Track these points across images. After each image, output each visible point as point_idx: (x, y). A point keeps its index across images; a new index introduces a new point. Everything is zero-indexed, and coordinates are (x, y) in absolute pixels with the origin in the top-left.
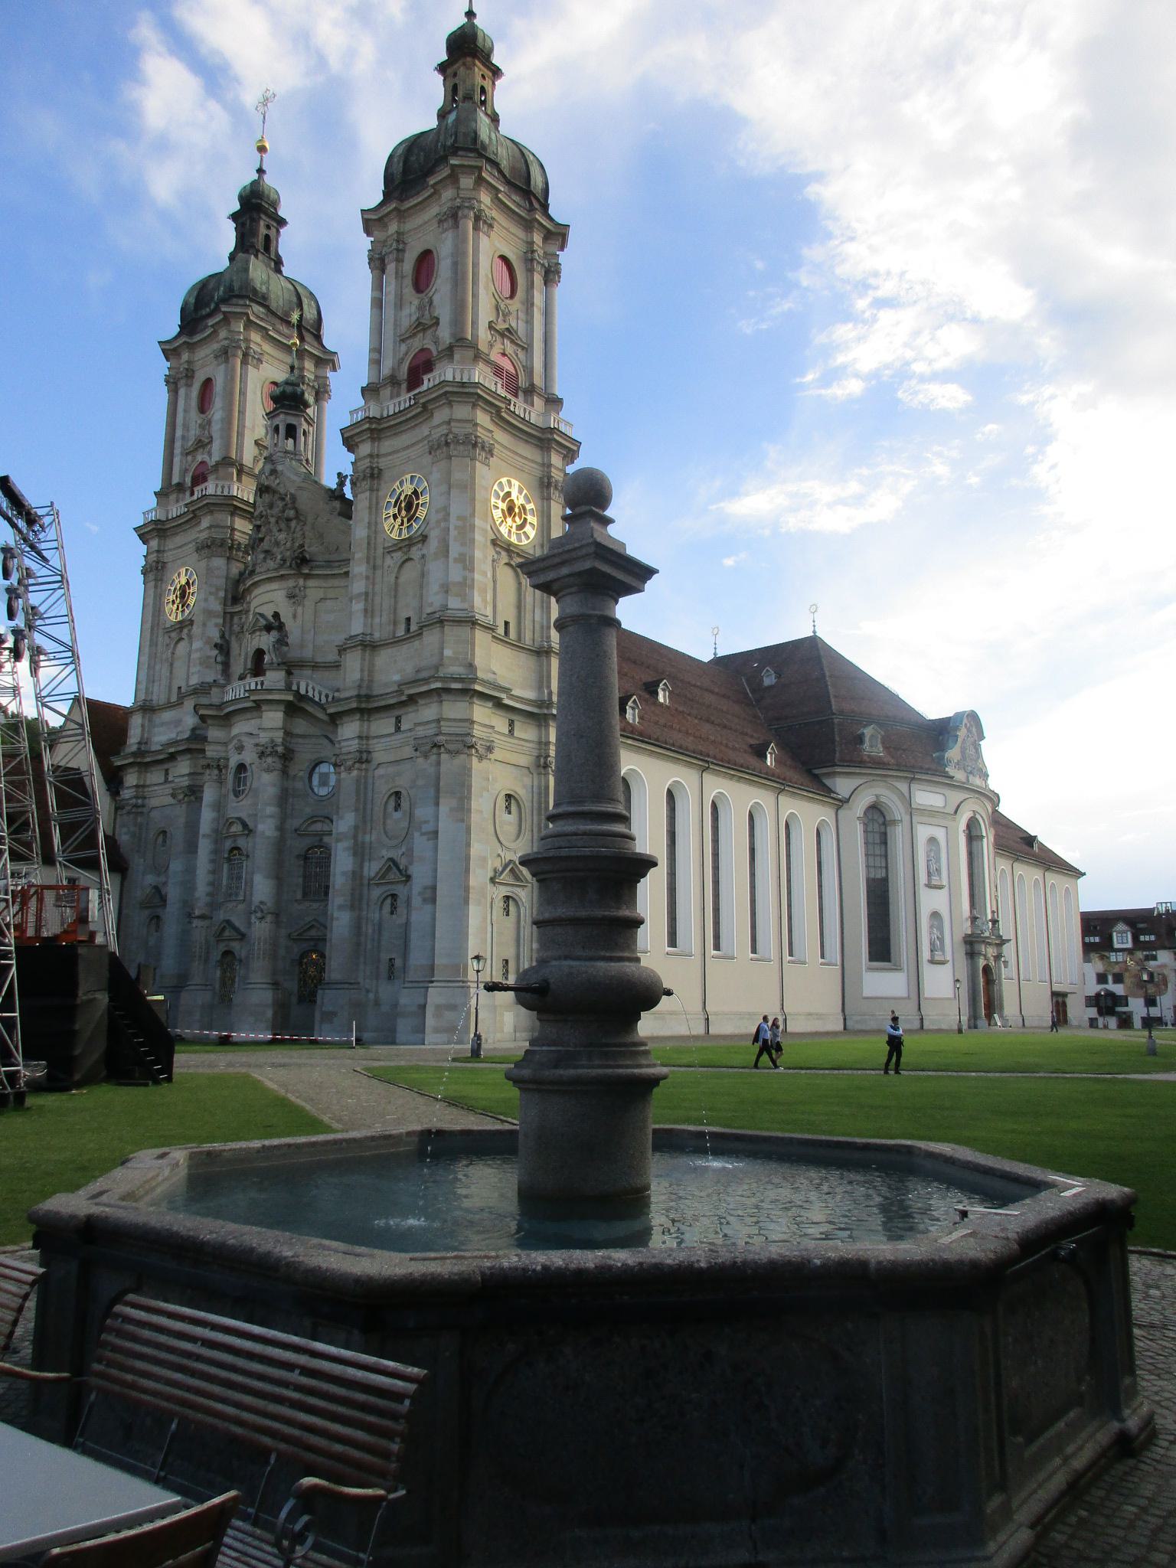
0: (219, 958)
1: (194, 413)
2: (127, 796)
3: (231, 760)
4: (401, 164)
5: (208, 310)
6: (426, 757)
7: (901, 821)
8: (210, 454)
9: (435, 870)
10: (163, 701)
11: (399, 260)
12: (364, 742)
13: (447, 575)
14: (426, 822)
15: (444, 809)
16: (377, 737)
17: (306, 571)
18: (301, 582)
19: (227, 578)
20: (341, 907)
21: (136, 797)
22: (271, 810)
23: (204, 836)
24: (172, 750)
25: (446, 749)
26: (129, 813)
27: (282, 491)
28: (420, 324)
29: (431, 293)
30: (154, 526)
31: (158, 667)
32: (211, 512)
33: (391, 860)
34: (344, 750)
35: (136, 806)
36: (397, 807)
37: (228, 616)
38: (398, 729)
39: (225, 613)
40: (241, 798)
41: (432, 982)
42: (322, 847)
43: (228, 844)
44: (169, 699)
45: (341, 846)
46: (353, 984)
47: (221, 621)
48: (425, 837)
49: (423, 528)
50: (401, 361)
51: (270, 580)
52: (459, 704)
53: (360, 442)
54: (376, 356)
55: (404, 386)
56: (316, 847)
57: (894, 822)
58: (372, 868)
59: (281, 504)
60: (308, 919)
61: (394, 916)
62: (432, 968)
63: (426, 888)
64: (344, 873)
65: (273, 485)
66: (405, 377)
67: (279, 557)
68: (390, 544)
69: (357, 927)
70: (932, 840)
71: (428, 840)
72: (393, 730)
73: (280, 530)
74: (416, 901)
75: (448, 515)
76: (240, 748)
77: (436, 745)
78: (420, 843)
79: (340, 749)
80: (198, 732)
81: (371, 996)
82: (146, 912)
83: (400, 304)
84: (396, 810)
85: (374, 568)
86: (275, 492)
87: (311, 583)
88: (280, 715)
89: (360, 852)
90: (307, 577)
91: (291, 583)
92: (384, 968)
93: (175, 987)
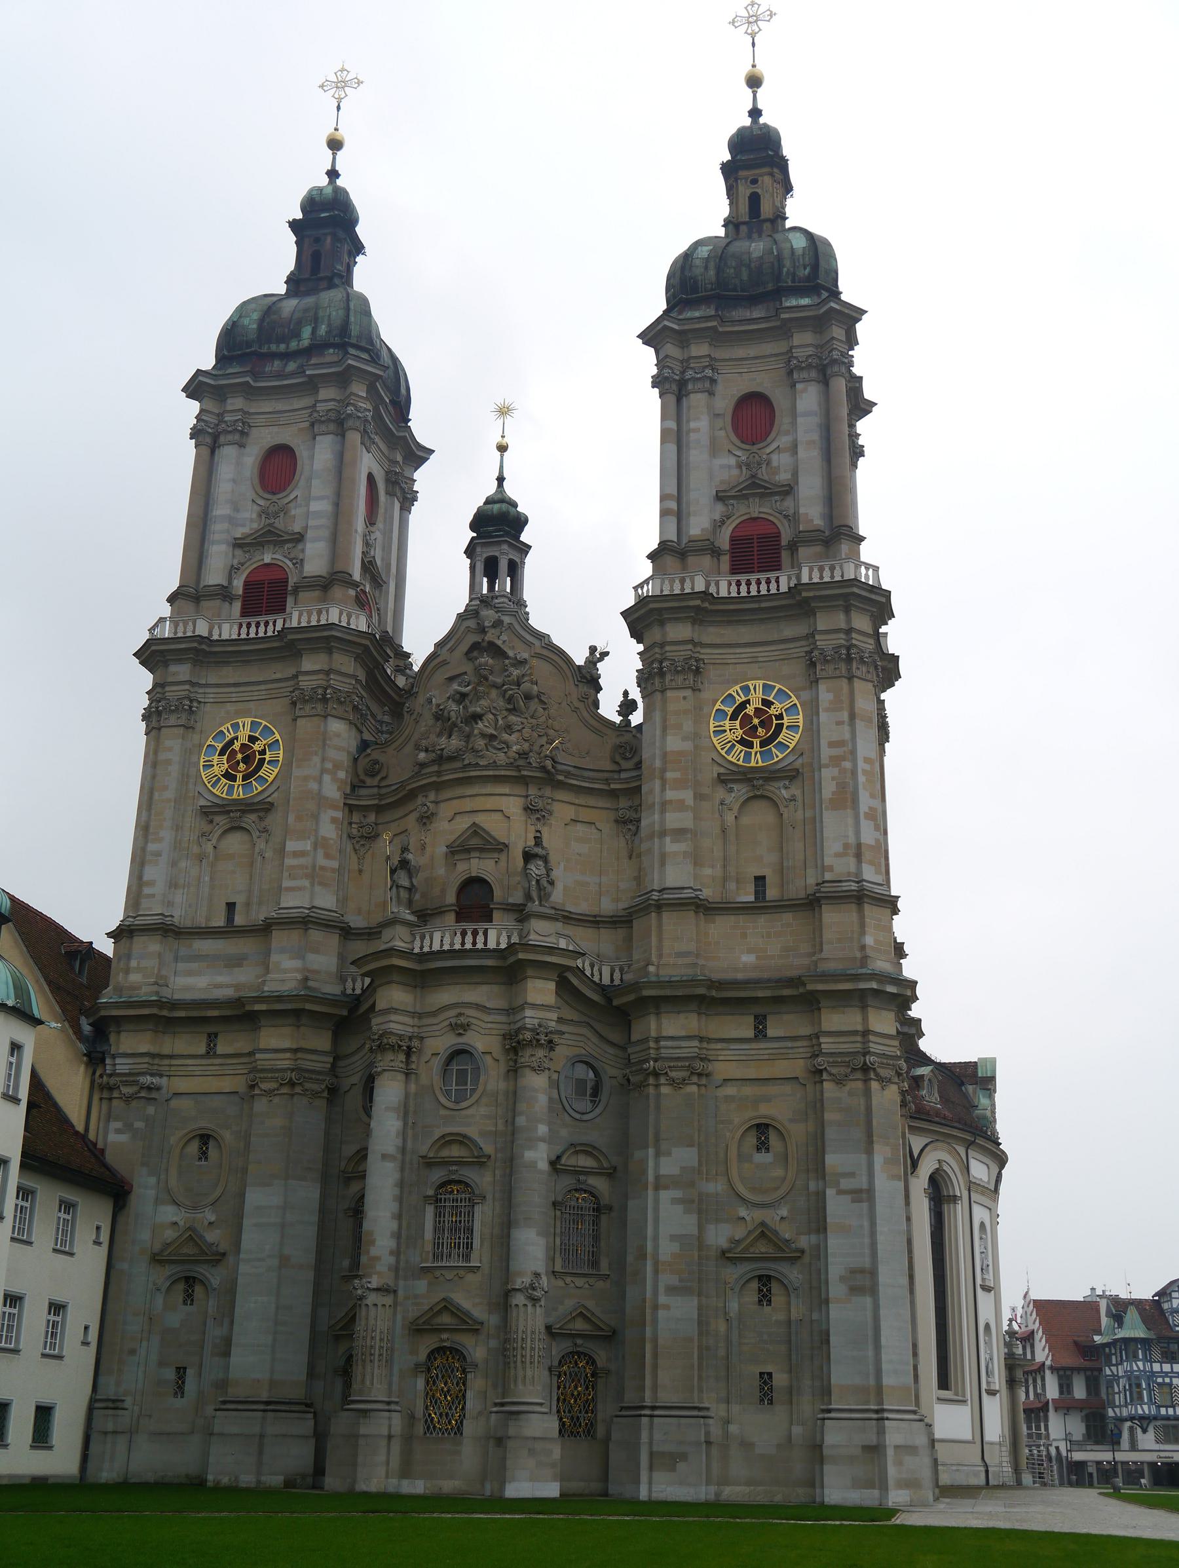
0: (422, 1357)
2: (120, 1069)
3: (429, 1042)
4: (712, 273)
5: (282, 347)
6: (839, 1082)
7: (961, 1197)
8: (299, 563)
9: (873, 1245)
11: (711, 393)
12: (705, 1045)
13: (858, 833)
14: (852, 1175)
15: (878, 1160)
17: (561, 778)
18: (548, 792)
19: (348, 752)
20: (671, 1290)
21: (152, 1075)
22: (542, 1129)
23: (384, 1157)
24: (257, 1007)
25: (877, 1075)
26: (128, 1099)
27: (511, 653)
28: (754, 485)
29: (768, 450)
30: (195, 645)
31: (183, 864)
32: (330, 651)
33: (763, 1224)
34: (664, 1052)
35: (149, 1089)
37: (347, 809)
38: (760, 1034)
39: (344, 804)
40: (464, 1104)
41: (829, 1411)
42: (585, 1191)
43: (438, 1175)
44: (208, 919)
45: (665, 1195)
46: (699, 1412)
48: (848, 1198)
49: (791, 759)
50: (719, 524)
51: (497, 779)
52: (884, 1013)
53: (670, 619)
54: (673, 505)
55: (726, 559)
56: (576, 1190)
57: (954, 1199)
58: (719, 1236)
59: (516, 672)
60: (569, 1304)
61: (767, 1309)
62: (879, 1389)
63: (853, 1271)
64: (673, 1238)
65: (499, 643)
66: (726, 546)
67: (515, 748)
68: (722, 770)
69: (702, 1323)
70: (982, 1225)
71: (853, 1201)
72: (750, 1033)
73: (514, 710)
74: (836, 1289)
75: (853, 752)
76: (459, 1028)
77: (865, 1069)
78: (837, 1207)
79: (658, 1049)
80: (310, 983)
81: (733, 1428)
82: (169, 1270)
83: (714, 450)
84: (759, 1150)
85: (699, 797)
86: (504, 655)
87: (561, 795)
88: (552, 986)
90: (560, 785)
91: (533, 791)
93: (268, 1403)
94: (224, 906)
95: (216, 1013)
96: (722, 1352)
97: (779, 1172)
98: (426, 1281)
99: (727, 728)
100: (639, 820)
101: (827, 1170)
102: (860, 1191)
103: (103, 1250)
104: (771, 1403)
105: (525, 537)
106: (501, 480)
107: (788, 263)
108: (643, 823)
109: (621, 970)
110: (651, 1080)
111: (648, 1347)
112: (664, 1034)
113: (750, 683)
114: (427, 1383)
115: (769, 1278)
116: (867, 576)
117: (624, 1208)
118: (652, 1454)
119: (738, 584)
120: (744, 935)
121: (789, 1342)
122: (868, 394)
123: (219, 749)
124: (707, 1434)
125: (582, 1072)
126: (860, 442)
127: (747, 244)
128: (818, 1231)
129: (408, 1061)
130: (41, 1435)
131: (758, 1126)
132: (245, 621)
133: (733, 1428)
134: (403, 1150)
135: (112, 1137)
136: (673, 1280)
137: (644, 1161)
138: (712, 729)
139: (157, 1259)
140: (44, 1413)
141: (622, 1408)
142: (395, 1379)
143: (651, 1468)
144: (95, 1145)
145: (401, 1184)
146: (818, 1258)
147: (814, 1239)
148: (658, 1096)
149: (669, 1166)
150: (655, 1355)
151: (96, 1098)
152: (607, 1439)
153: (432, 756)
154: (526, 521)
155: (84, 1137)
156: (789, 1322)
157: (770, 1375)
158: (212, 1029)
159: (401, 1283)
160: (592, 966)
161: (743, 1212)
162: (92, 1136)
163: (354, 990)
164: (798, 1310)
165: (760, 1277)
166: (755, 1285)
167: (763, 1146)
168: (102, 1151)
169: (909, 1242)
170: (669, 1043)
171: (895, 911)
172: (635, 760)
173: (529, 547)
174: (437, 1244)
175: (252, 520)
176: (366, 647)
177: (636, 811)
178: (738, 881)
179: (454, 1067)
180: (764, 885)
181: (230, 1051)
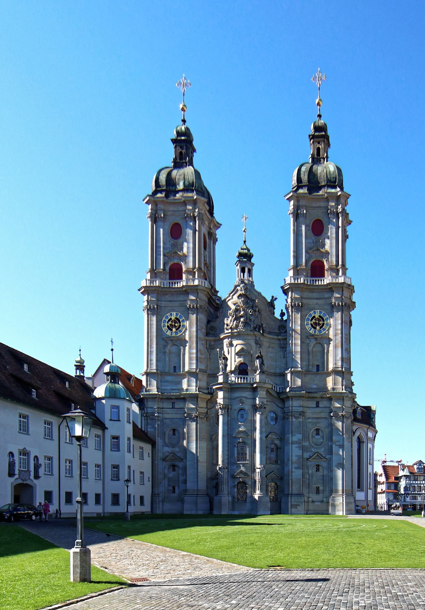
0: (236, 484)
1: (169, 238)
10: (167, 370)
16: (308, 407)
20: (296, 468)
36: (318, 434)
38: (317, 406)
45: (294, 446)
47: (204, 342)
63: (339, 464)
64: (296, 456)
66: (310, 268)
72: (315, 406)
81: (310, 499)
84: (317, 435)
89: (304, 449)
92: (315, 490)
94: (173, 367)
95: (174, 397)
96: (308, 482)
97: (321, 440)
98: (236, 466)
99: (310, 323)
100: (286, 348)
101: (333, 440)
102: (341, 445)
103: (150, 459)
104: (319, 493)
105: (253, 260)
106: (245, 242)
107: (329, 177)
108: (288, 349)
109: (282, 388)
110: (290, 417)
111: (290, 481)
112: (294, 406)
113: (316, 311)
114: (237, 490)
115: (319, 465)
116: (348, 281)
117: (284, 448)
118: (291, 505)
119: (313, 280)
120: (314, 380)
121: (323, 480)
122: (351, 218)
123: (167, 321)
124: (304, 500)
125: (272, 415)
126: (348, 234)
127: (317, 167)
128: (331, 455)
129: (228, 412)
130: (142, 503)
131: (317, 429)
132: (171, 281)
133: (310, 499)
134: (228, 435)
135: (149, 430)
136: (296, 466)
137: (288, 438)
138: (306, 323)
139: (164, 460)
140: (142, 498)
141: (284, 495)
142: (229, 489)
143: (291, 508)
144: (144, 431)
145: (228, 443)
146: (331, 461)
147: (330, 456)
148: (292, 421)
149: (295, 439)
150: (292, 483)
151: (143, 418)
152: (281, 502)
153: (229, 327)
154: (253, 256)
155: (141, 429)
156: (323, 475)
157: (319, 487)
158: (173, 401)
159: (229, 466)
160: (274, 387)
161: (313, 450)
162: (143, 429)
163: (211, 391)
164: (325, 472)
165: (317, 465)
166: (315, 467)
167: (318, 434)
168: (147, 433)
169: (352, 456)
170: (295, 408)
171: (352, 375)
172: (285, 330)
173: (254, 264)
174: (238, 457)
175: (169, 248)
176: (208, 292)
177: (285, 345)
178: (312, 366)
179: (240, 413)
180: (319, 367)
181: (178, 407)
